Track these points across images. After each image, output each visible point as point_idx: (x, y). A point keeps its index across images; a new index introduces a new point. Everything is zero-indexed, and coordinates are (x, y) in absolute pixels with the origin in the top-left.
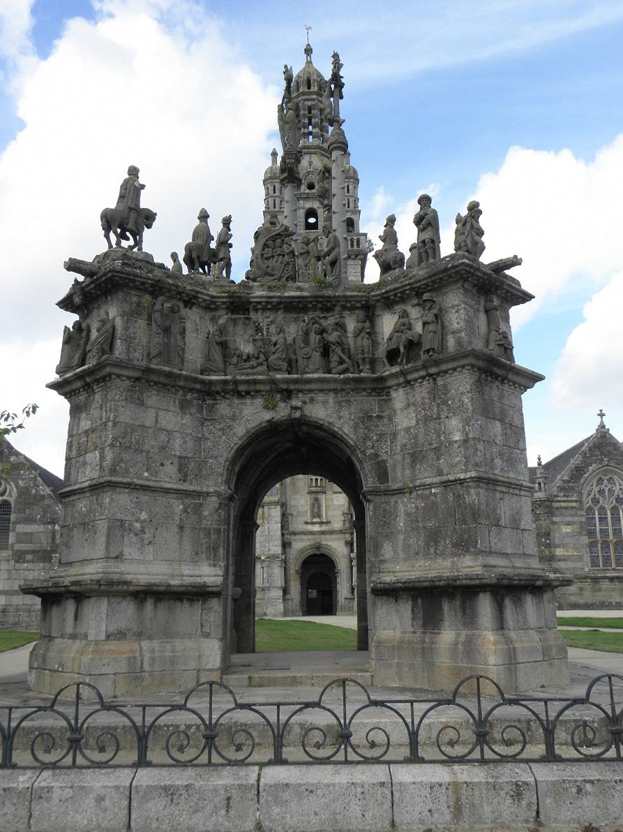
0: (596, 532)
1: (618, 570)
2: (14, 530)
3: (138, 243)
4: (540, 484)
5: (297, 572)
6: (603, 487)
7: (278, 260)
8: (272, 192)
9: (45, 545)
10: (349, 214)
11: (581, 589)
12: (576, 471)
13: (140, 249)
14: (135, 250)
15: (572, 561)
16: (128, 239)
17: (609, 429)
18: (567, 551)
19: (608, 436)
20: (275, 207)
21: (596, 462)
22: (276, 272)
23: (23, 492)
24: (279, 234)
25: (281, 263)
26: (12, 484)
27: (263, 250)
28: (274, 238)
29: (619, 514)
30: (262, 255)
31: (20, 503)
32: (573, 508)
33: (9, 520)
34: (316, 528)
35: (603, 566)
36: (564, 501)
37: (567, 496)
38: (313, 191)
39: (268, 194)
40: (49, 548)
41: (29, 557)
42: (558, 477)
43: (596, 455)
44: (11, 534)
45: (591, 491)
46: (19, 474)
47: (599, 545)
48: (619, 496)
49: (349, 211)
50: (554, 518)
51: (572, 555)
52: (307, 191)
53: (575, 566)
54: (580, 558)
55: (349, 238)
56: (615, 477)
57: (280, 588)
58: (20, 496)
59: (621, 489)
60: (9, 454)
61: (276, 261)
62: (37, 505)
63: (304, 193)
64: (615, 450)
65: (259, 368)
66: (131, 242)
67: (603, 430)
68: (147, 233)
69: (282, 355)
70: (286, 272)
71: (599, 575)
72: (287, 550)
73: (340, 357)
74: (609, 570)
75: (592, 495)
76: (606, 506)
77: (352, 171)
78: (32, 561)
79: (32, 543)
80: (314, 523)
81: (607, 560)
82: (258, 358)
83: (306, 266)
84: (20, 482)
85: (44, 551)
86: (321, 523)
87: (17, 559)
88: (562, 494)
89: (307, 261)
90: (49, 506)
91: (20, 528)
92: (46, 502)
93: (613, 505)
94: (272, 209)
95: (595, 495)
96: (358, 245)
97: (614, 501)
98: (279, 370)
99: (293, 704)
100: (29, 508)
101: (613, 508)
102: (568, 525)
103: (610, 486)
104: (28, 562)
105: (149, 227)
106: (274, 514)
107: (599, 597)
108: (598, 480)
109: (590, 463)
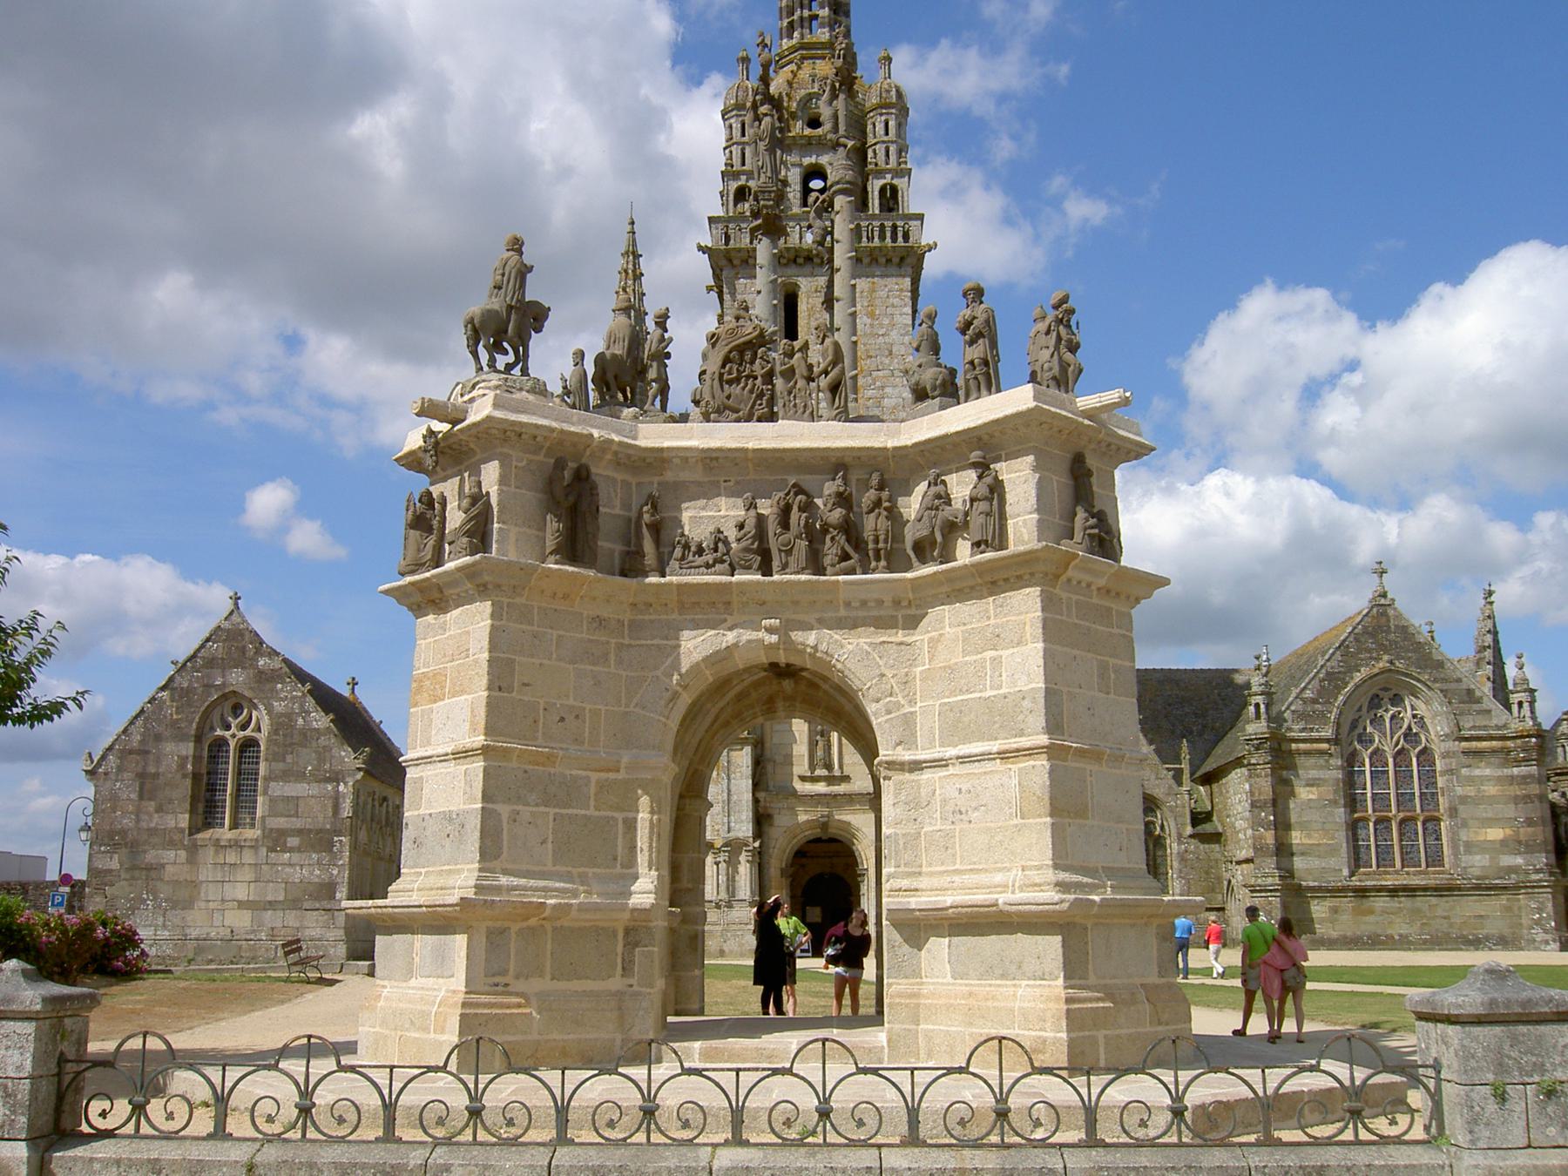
0: (1366, 801)
1: (1408, 873)
2: (265, 793)
3: (522, 358)
4: (1257, 706)
5: (783, 872)
7: (746, 385)
8: (739, 134)
9: (321, 819)
10: (889, 176)
11: (1335, 910)
12: (1330, 681)
13: (525, 372)
14: (517, 371)
15: (1319, 856)
16: (506, 353)
17: (1393, 600)
18: (1309, 836)
19: (1391, 612)
20: (743, 164)
21: (1367, 665)
22: (742, 406)
23: (282, 725)
24: (750, 342)
25: (751, 392)
26: (261, 707)
27: (723, 366)
28: (741, 349)
30: (721, 375)
31: (276, 743)
32: (1322, 753)
33: (257, 774)
34: (821, 788)
35: (1378, 867)
36: (1304, 741)
37: (1312, 730)
38: (819, 131)
39: (731, 139)
40: (328, 827)
41: (293, 841)
43: (1369, 651)
44: (260, 799)
46: (273, 690)
47: (1371, 825)
48: (1410, 728)
49: (889, 171)
51: (1319, 845)
52: (808, 131)
53: (1323, 865)
54: (1332, 851)
55: (888, 224)
57: (751, 904)
58: (275, 730)
59: (1414, 716)
60: (255, 653)
61: (743, 388)
62: (306, 747)
63: (803, 137)
64: (1405, 639)
65: (718, 567)
66: (511, 358)
67: (1383, 601)
68: (535, 341)
69: (753, 544)
70: (757, 407)
71: (1368, 883)
72: (766, 828)
73: (843, 549)
74: (1388, 873)
76: (1386, 748)
77: (893, 93)
78: (299, 850)
79: (298, 817)
80: (814, 779)
81: (1384, 857)
82: (716, 550)
83: (790, 393)
84: (275, 704)
85: (320, 831)
86: (830, 780)
87: (270, 845)
88: (1301, 725)
89: (792, 383)
90: (327, 749)
91: (278, 789)
92: (323, 741)
93: (1399, 747)
94: (737, 167)
96: (906, 237)
97: (1402, 740)
99: (757, 1069)
100: (292, 753)
101: (1399, 753)
102: (1312, 785)
104: (291, 850)
105: (538, 330)
106: (739, 761)
107: (1368, 925)
108: (1372, 699)
109: (1357, 665)
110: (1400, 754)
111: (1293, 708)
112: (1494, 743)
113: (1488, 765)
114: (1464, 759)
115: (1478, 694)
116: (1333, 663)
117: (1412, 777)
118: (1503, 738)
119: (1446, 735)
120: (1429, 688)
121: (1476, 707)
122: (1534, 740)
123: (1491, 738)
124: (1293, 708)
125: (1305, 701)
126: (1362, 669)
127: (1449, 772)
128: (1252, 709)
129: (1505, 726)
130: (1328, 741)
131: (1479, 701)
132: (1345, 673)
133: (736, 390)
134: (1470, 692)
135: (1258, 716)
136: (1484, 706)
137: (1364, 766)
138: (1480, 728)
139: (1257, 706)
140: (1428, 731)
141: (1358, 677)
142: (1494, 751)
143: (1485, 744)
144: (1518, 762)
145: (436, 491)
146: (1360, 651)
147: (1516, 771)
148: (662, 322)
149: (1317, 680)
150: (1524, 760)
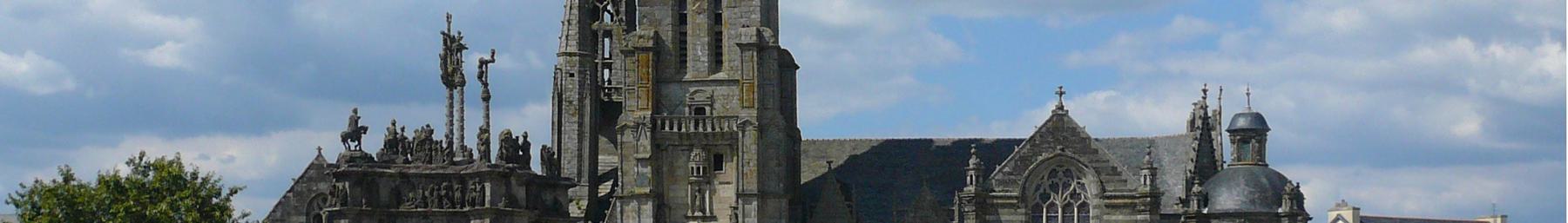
4: (971, 176)
6: (1056, 180)
21: (1047, 152)
29: (1073, 212)
32: (1012, 206)
37: (1007, 191)
42: (998, 168)
45: (1040, 186)
48: (1075, 190)
50: (987, 217)
56: (1073, 169)
65: (413, 206)
75: (1042, 191)
76: (1057, 202)
93: (1066, 202)
95: (1045, 190)
98: (421, 207)
103: (1065, 179)
108: (1051, 173)
109: (1040, 152)
110: (1067, 207)
111: (996, 178)
112: (1126, 201)
113: (1121, 213)
114: (1107, 211)
115: (1119, 170)
116: (1025, 150)
117: (1073, 219)
118: (1133, 197)
119: (1096, 195)
120: (1087, 167)
121: (1117, 177)
122: (1149, 199)
123: (1123, 197)
124: (996, 178)
125: (1004, 174)
126: (1043, 154)
127: (1097, 217)
128: (969, 178)
129: (1135, 190)
130: (1016, 198)
131: (1119, 174)
132: (1031, 157)
133: (420, 154)
134: (1114, 169)
135: (971, 183)
136: (1123, 178)
137: (1058, 212)
138: (1119, 191)
139: (971, 176)
140: (1086, 192)
141: (1040, 158)
142: (1125, 206)
143: (1120, 201)
144: (1140, 212)
145: (337, 184)
146: (1042, 143)
147: (1139, 217)
148: (403, 129)
149: (1013, 162)
150: (1143, 211)
